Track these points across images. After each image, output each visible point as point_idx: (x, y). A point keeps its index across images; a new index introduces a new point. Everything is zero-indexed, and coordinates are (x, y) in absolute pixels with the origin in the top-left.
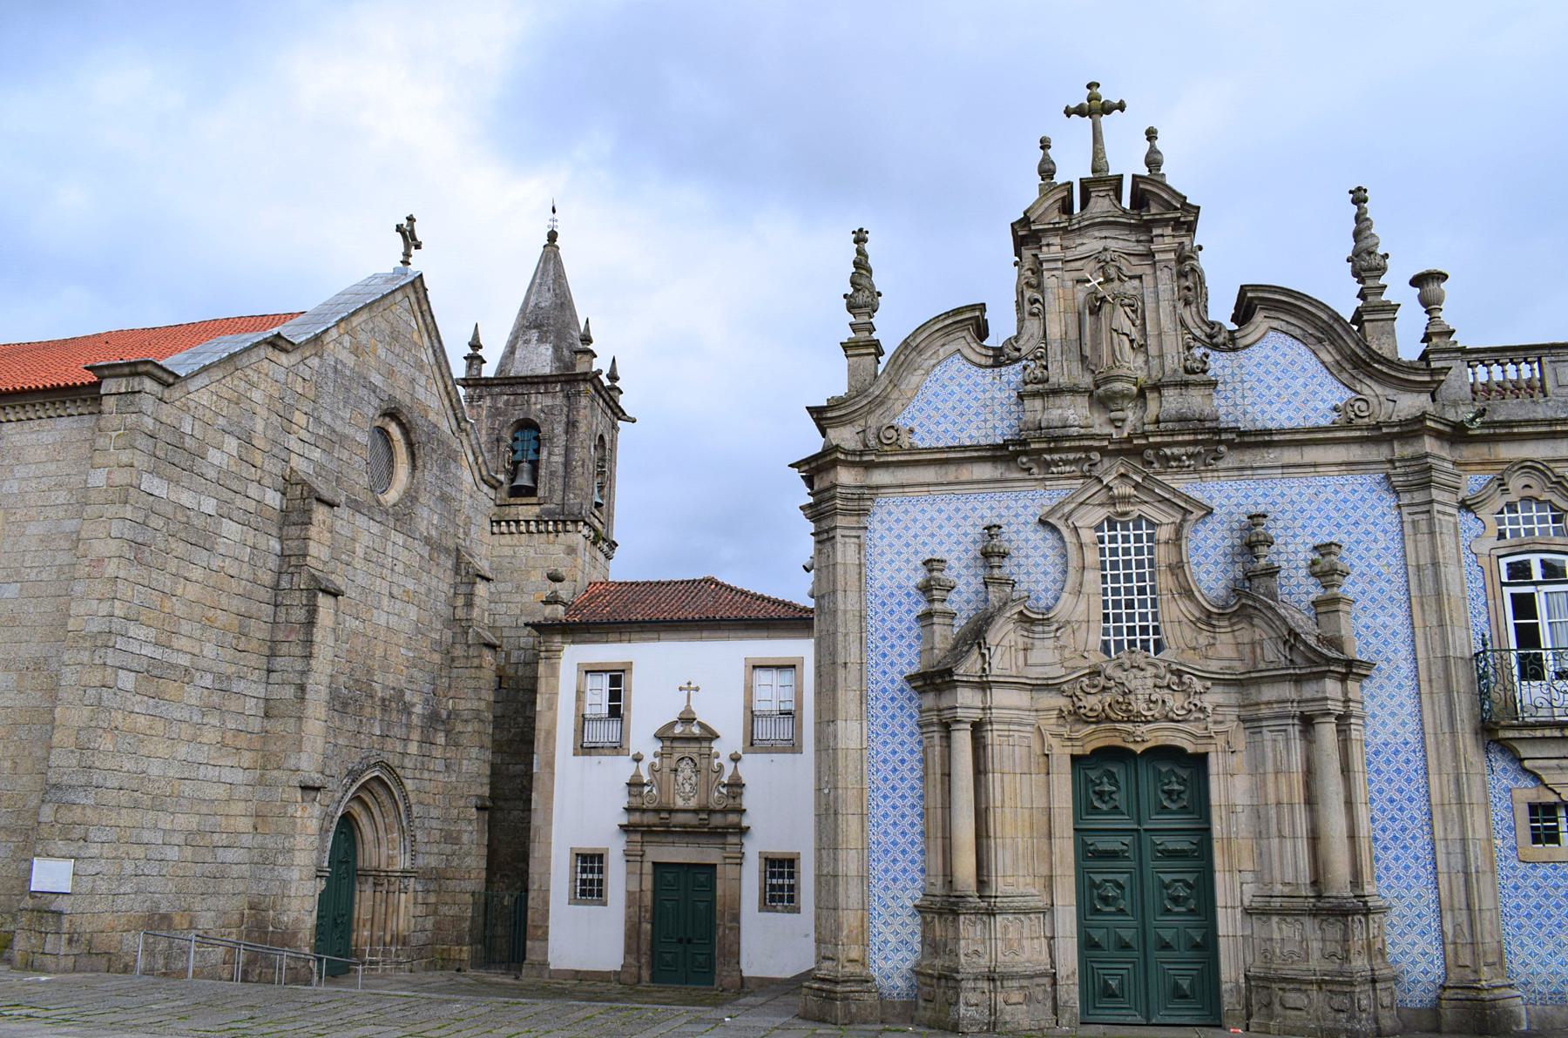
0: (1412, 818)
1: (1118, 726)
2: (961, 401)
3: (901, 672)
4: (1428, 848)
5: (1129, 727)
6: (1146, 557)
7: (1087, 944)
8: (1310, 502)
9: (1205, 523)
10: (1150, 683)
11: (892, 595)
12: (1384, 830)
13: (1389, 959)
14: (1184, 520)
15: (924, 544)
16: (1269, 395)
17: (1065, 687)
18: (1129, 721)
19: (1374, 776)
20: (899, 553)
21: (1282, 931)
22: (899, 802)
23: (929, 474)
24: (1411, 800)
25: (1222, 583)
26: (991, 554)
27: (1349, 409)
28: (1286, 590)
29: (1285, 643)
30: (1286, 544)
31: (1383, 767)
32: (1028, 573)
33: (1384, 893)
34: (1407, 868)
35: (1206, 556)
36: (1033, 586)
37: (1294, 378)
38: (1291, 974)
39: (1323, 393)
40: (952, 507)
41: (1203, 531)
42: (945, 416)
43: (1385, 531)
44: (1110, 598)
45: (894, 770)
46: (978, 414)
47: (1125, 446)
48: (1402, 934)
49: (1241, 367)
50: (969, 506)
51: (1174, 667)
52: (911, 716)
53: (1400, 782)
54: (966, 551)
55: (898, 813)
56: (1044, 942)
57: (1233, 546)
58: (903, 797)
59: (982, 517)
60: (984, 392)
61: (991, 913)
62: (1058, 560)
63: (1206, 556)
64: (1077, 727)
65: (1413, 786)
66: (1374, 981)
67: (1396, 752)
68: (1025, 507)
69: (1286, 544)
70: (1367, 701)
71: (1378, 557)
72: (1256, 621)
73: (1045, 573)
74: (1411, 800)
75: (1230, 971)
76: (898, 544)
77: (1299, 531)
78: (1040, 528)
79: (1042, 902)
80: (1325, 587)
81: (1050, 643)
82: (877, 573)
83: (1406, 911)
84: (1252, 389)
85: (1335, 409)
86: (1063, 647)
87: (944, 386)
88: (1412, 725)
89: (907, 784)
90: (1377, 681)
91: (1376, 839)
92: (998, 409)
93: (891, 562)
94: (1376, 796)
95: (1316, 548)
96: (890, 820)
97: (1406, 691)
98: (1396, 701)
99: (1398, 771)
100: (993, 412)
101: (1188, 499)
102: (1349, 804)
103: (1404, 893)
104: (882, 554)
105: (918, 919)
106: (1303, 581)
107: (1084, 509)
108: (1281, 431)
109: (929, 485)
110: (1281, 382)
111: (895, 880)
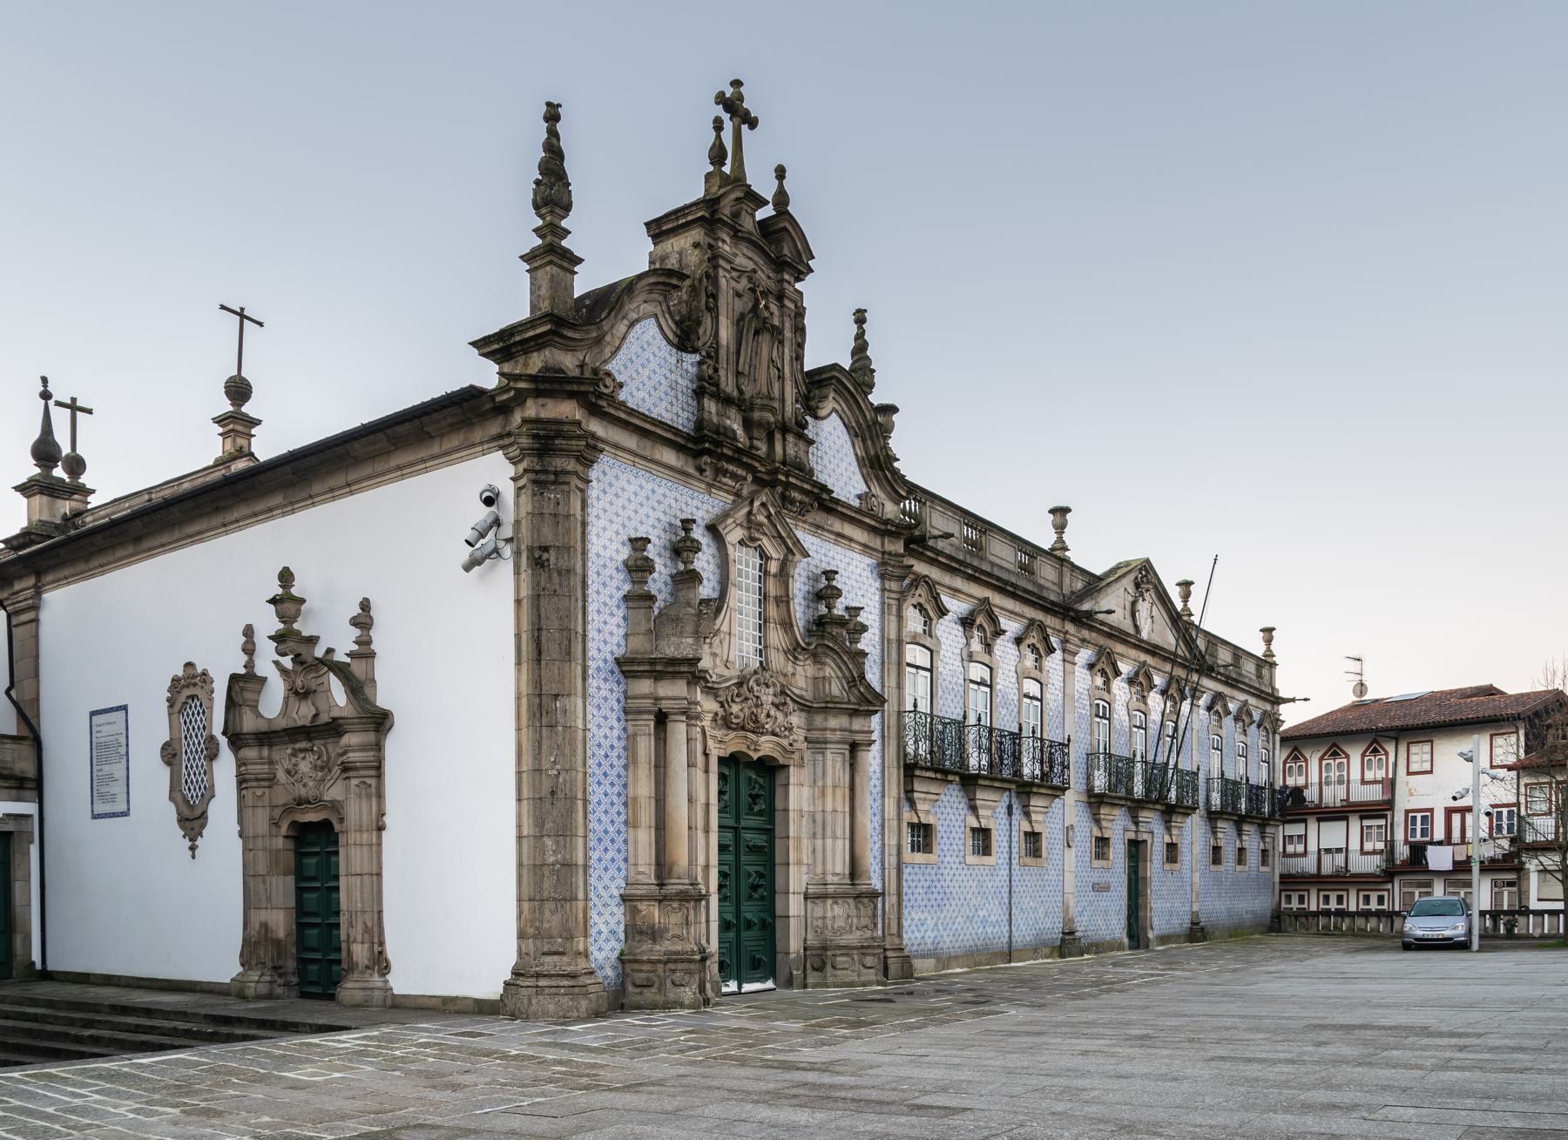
3: (612, 653)
21: (837, 912)
38: (843, 943)
45: (606, 756)
55: (608, 800)
58: (612, 784)
96: (603, 808)
110: (834, 458)
111: (606, 869)
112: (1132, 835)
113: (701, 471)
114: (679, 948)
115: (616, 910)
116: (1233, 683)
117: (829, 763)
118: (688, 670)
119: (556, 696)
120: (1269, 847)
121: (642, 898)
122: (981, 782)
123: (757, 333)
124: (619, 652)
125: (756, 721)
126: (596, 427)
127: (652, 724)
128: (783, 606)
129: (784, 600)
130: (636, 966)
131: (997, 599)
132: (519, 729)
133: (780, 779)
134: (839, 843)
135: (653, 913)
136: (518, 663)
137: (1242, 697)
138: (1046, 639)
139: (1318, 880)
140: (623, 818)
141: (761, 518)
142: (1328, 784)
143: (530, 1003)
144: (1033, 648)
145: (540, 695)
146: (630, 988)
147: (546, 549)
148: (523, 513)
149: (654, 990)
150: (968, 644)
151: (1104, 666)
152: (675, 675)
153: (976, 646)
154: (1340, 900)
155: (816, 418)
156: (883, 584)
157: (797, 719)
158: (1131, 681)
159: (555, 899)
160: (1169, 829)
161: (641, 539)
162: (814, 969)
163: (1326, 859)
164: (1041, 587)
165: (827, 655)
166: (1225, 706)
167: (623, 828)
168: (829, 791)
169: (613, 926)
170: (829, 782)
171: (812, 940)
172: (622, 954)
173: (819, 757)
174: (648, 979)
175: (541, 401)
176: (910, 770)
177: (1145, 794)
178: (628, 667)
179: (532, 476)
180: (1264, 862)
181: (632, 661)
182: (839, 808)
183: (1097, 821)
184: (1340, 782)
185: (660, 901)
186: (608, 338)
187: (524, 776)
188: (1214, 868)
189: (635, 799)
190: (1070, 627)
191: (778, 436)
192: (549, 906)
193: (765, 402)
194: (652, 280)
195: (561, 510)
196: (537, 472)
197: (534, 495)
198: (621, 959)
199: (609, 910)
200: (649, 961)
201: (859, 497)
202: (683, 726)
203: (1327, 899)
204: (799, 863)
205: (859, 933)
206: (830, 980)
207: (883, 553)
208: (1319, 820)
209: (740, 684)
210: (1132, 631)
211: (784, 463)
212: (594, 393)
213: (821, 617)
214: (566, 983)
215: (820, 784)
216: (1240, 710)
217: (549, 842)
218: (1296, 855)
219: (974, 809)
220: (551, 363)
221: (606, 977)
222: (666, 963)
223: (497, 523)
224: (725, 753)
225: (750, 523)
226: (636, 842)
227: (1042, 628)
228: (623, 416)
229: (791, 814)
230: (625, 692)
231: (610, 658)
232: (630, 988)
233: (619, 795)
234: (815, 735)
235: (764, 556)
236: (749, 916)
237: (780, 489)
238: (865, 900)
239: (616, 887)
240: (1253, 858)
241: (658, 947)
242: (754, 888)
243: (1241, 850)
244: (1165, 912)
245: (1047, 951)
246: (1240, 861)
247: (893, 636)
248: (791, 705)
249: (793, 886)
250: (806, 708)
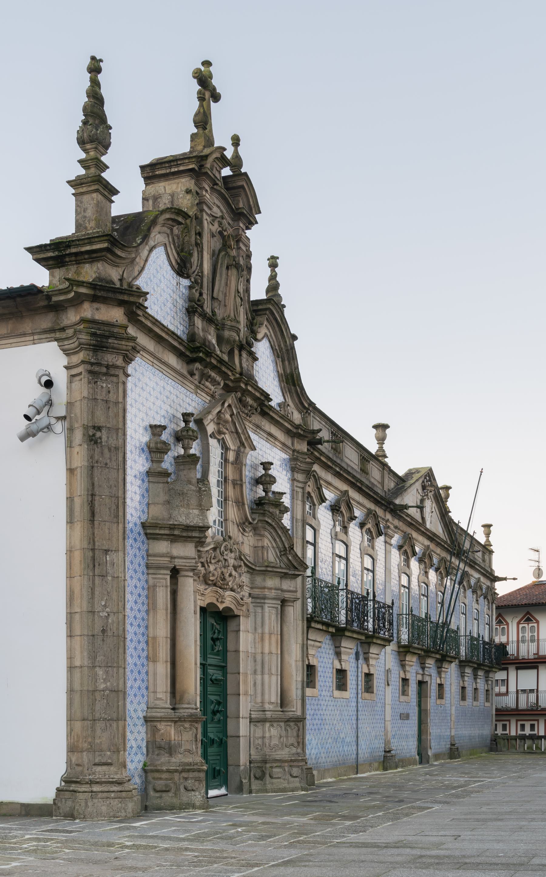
21: (273, 733)
38: (278, 757)
112: (420, 678)
113: (192, 374)
114: (191, 760)
116: (472, 564)
117: (267, 615)
118: (195, 534)
119: (106, 551)
120: (490, 688)
121: (161, 720)
122: (347, 634)
123: (227, 268)
124: (144, 518)
125: (224, 579)
126: (132, 331)
127: (168, 577)
128: (238, 488)
129: (238, 484)
130: (157, 775)
131: (353, 494)
132: (70, 577)
133: (231, 626)
134: (274, 678)
135: (170, 732)
136: (70, 521)
137: (477, 575)
138: (377, 525)
139: (516, 713)
140: (145, 653)
141: (228, 417)
142: (523, 641)
143: (87, 806)
144: (369, 532)
145: (93, 550)
146: (152, 793)
147: (99, 429)
148: (77, 396)
149: (170, 794)
150: (334, 526)
151: (406, 549)
152: (187, 539)
153: (338, 529)
154: (532, 727)
155: (256, 340)
156: (293, 475)
157: (245, 579)
158: (420, 561)
159: (105, 719)
160: (439, 673)
161: (160, 426)
162: (256, 778)
163: (523, 698)
164: (373, 484)
165: (265, 529)
166: (469, 581)
168: (267, 637)
169: (139, 742)
170: (267, 630)
172: (145, 765)
173: (259, 610)
174: (166, 786)
175: (96, 305)
176: (310, 621)
177: (432, 644)
178: (151, 530)
179: (89, 367)
180: (487, 700)
181: (155, 526)
182: (274, 650)
183: (403, 666)
184: (532, 641)
185: (175, 722)
186: (137, 260)
187: (77, 617)
188: (462, 703)
189: (155, 638)
190: (389, 516)
191: (236, 352)
192: (100, 725)
193: (233, 324)
194: (167, 216)
195: (112, 397)
196: (92, 364)
197: (89, 383)
198: (145, 771)
200: (168, 771)
201: (279, 405)
202: (191, 580)
203: (523, 727)
204: (246, 694)
205: (287, 750)
206: (269, 787)
207: (294, 451)
208: (517, 669)
209: (214, 549)
210: (420, 520)
211: (241, 374)
212: (131, 300)
213: (261, 499)
214: (115, 788)
215: (260, 631)
216: (476, 584)
217: (100, 672)
218: (499, 694)
219: (338, 654)
220: (103, 275)
222: (182, 772)
223: (50, 403)
224: (204, 605)
225: (219, 419)
226: (155, 674)
227: (376, 516)
228: (149, 324)
229: (242, 655)
230: (147, 551)
231: (138, 522)
232: (152, 793)
233: (143, 634)
234: (256, 592)
235: (225, 447)
236: (211, 735)
237: (239, 394)
238: (292, 724)
240: (482, 696)
241: (173, 760)
242: (214, 713)
243: (476, 689)
244: (439, 735)
245: (376, 765)
246: (475, 698)
247: (299, 517)
248: (244, 569)
249: (244, 712)
250: (251, 571)
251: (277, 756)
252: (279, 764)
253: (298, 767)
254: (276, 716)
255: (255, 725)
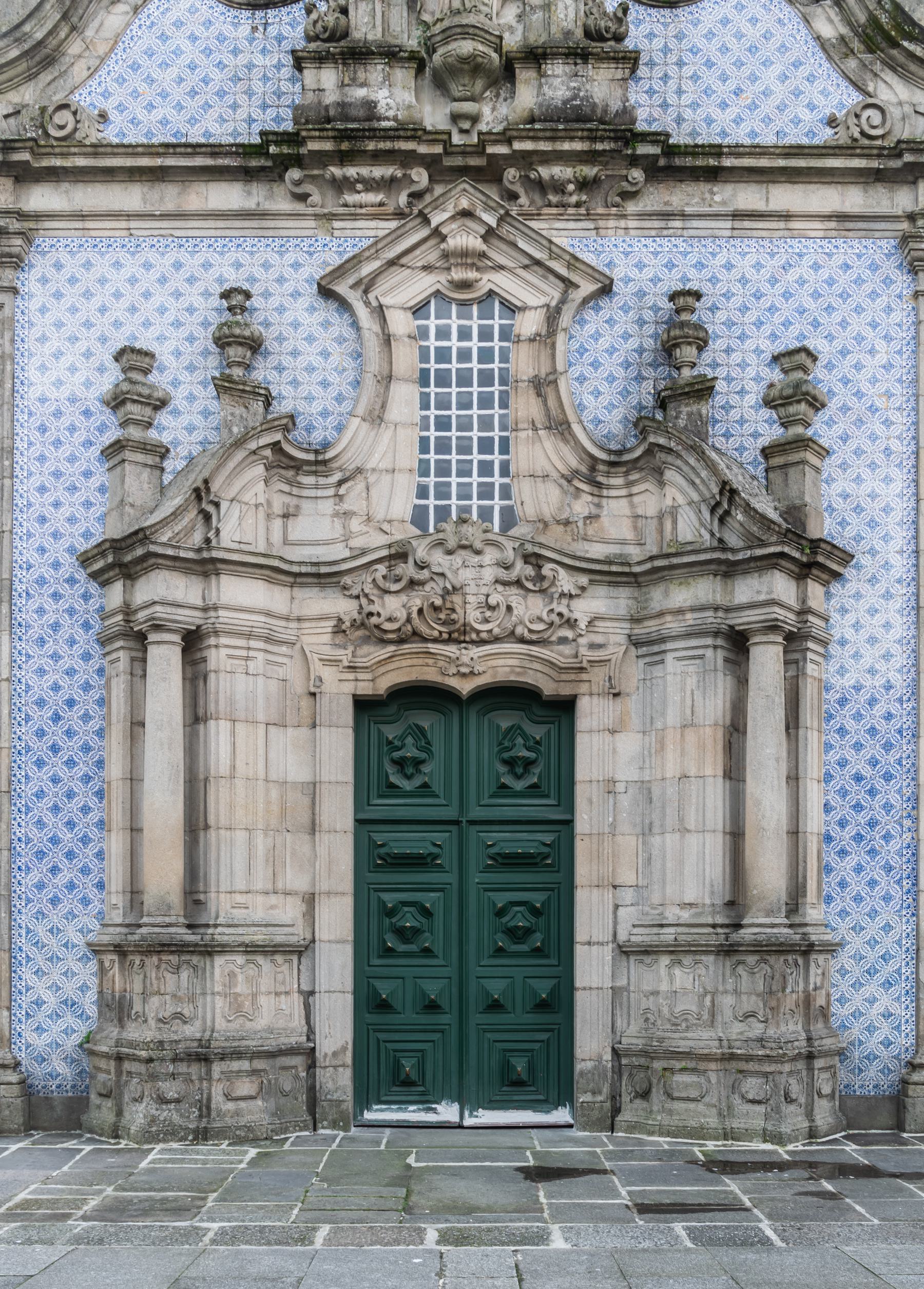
0: (888, 807)
1: (433, 647)
2: (192, 67)
4: (907, 853)
5: (451, 650)
6: (496, 366)
7: (370, 1004)
8: (773, 281)
9: (597, 309)
10: (489, 574)
11: (58, 414)
12: (842, 824)
13: (835, 1023)
14: (563, 301)
15: (117, 324)
16: (723, 90)
17: (347, 580)
18: (450, 640)
19: (834, 738)
20: (73, 339)
21: (677, 985)
22: (63, 772)
23: (130, 197)
24: (888, 777)
25: (618, 414)
26: (238, 340)
27: (852, 121)
28: (720, 429)
29: (713, 510)
30: (728, 351)
31: (850, 725)
32: (295, 383)
33: (835, 921)
34: (872, 883)
35: (595, 365)
36: (302, 406)
37: (767, 63)
38: (684, 1046)
39: (813, 92)
40: (169, 259)
41: (594, 320)
42: (164, 95)
43: (887, 338)
44: (433, 434)
45: (56, 718)
46: (221, 94)
47: (474, 162)
48: (857, 985)
49: (680, 37)
50: (199, 259)
51: (530, 548)
52: (87, 626)
53: (873, 749)
54: (191, 339)
55: (61, 789)
56: (297, 1001)
57: (641, 351)
58: (71, 763)
59: (220, 280)
60: (235, 52)
61: (209, 951)
62: (349, 363)
63: (595, 365)
64: (366, 649)
65: (892, 757)
66: (810, 1057)
67: (872, 702)
68: (296, 266)
69: (728, 351)
70: (835, 617)
71: (874, 381)
72: (669, 474)
73: (325, 384)
74: (888, 777)
75: (591, 1044)
76: (72, 325)
77: (750, 330)
78: (320, 303)
79: (299, 934)
80: (784, 425)
81: (328, 506)
82: (32, 374)
83: (866, 951)
84: (695, 78)
85: (832, 122)
86: (348, 514)
87: (164, 37)
88: (901, 659)
89: (75, 743)
90: (852, 587)
91: (828, 838)
92: (258, 86)
93: (58, 355)
94: (836, 771)
95: (776, 359)
96: (47, 802)
97: (897, 603)
98: (879, 619)
99: (873, 731)
100: (249, 93)
101: (574, 262)
102: (794, 779)
103: (865, 921)
104: (43, 339)
105: (93, 966)
106: (750, 414)
107: (397, 276)
108: (737, 150)
109: (129, 216)
111: (55, 901)
115: (76, 967)
140: (94, 817)
167: (94, 833)
171: (632, 1035)
199: (61, 967)
221: (52, 1076)
239: (82, 925)
251: (682, 1043)
252: (691, 1064)
253: (766, 1075)
254: (689, 938)
255: (641, 961)
